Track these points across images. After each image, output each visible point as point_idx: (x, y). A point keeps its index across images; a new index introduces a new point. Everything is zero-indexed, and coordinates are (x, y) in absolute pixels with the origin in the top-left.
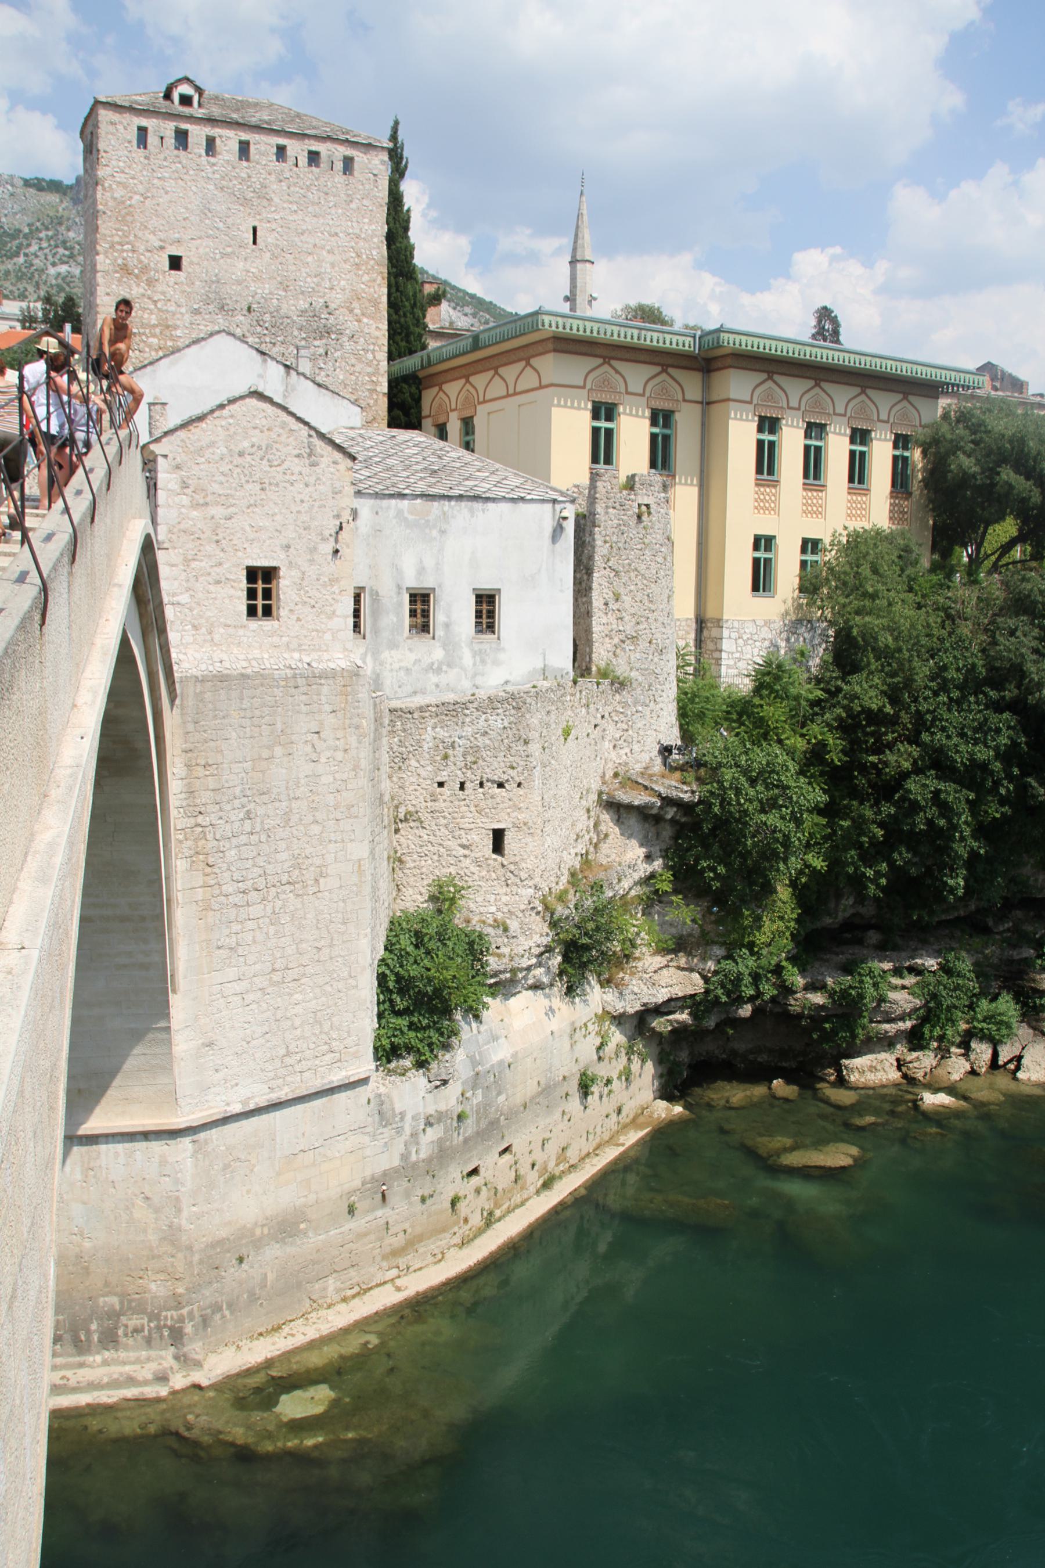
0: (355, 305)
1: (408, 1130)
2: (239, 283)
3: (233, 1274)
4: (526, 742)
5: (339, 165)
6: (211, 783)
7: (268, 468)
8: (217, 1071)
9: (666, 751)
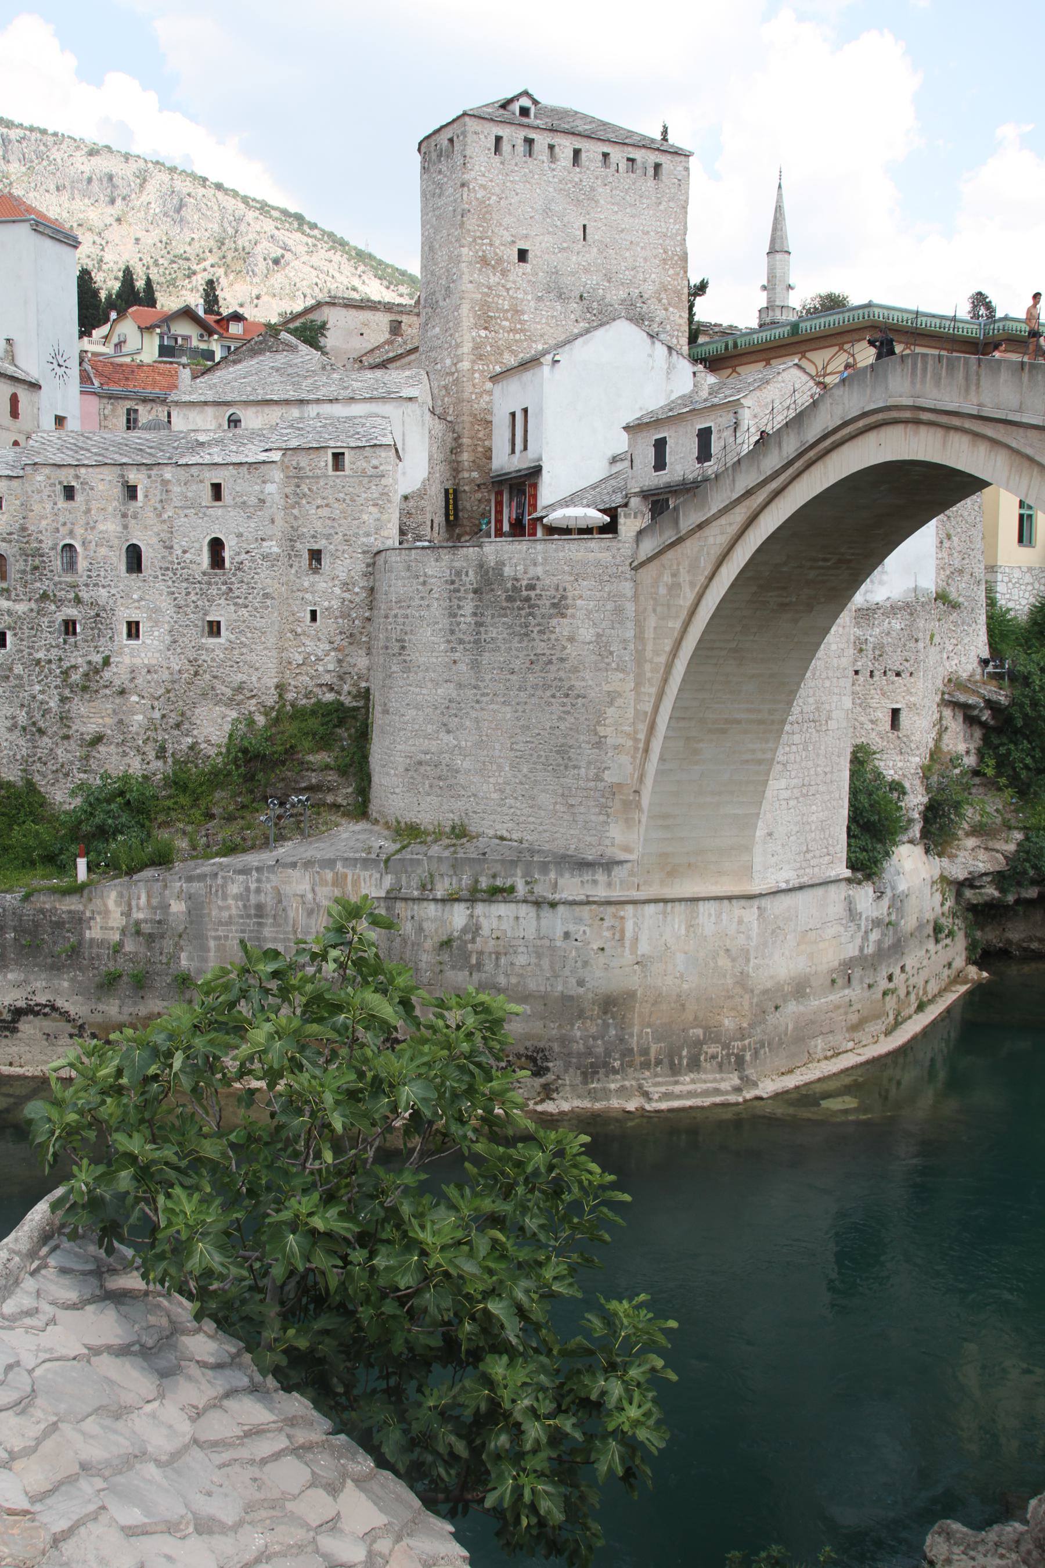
0: (663, 296)
1: (863, 929)
2: (573, 274)
3: (772, 1019)
4: (917, 641)
5: (651, 171)
9: (985, 662)
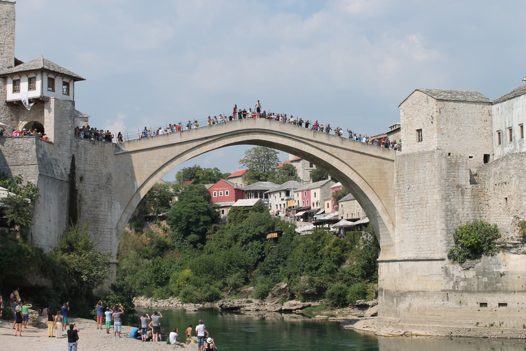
1: (455, 280)
6: (402, 179)
7: (419, 106)
8: (404, 248)
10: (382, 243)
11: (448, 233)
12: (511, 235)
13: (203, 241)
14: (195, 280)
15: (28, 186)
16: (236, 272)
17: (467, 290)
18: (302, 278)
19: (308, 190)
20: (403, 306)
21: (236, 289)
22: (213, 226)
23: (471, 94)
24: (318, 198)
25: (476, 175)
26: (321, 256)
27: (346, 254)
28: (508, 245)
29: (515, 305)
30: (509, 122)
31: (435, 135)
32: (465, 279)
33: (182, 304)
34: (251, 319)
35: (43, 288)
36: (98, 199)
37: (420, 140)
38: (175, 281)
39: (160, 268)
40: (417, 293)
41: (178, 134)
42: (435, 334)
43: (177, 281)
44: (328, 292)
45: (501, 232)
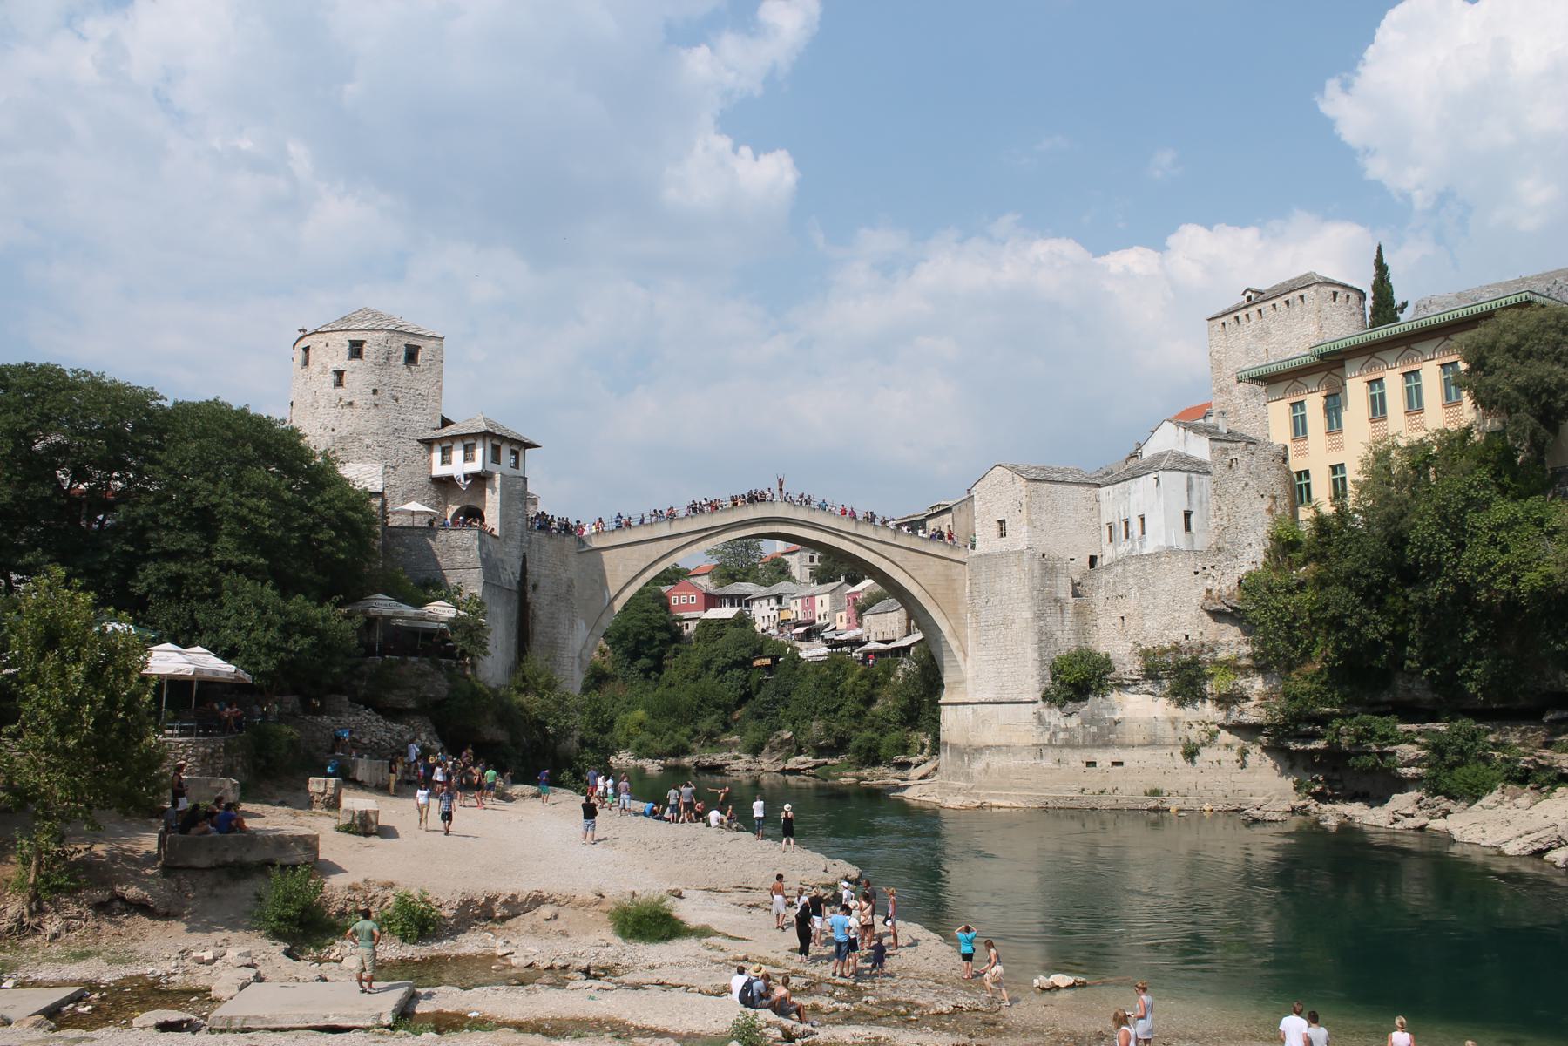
6: (977, 589)
10: (948, 677)
11: (1041, 666)
12: (1129, 668)
13: (659, 668)
14: (652, 725)
15: (471, 599)
16: (712, 713)
17: (1069, 744)
18: (814, 724)
19: (812, 596)
20: (978, 766)
21: (712, 740)
22: (674, 646)
23: (1071, 472)
24: (827, 608)
25: (1079, 584)
26: (842, 693)
27: (877, 691)
28: (1125, 682)
29: (1133, 765)
30: (1125, 512)
31: (1025, 528)
32: (1066, 729)
33: (635, 759)
34: (740, 782)
35: (498, 744)
36: (556, 616)
37: (1003, 534)
38: (622, 727)
39: (599, 708)
40: (998, 748)
41: (666, 524)
42: (1023, 805)
43: (626, 726)
44: (853, 744)
45: (1114, 664)
